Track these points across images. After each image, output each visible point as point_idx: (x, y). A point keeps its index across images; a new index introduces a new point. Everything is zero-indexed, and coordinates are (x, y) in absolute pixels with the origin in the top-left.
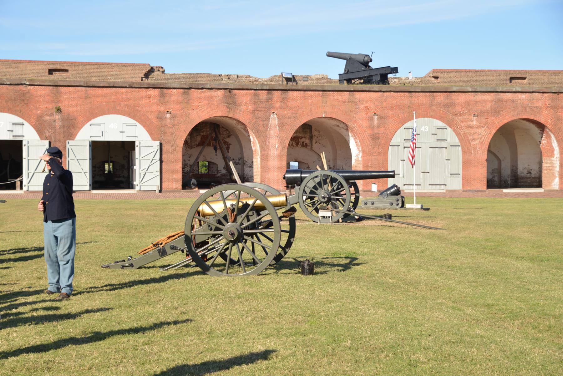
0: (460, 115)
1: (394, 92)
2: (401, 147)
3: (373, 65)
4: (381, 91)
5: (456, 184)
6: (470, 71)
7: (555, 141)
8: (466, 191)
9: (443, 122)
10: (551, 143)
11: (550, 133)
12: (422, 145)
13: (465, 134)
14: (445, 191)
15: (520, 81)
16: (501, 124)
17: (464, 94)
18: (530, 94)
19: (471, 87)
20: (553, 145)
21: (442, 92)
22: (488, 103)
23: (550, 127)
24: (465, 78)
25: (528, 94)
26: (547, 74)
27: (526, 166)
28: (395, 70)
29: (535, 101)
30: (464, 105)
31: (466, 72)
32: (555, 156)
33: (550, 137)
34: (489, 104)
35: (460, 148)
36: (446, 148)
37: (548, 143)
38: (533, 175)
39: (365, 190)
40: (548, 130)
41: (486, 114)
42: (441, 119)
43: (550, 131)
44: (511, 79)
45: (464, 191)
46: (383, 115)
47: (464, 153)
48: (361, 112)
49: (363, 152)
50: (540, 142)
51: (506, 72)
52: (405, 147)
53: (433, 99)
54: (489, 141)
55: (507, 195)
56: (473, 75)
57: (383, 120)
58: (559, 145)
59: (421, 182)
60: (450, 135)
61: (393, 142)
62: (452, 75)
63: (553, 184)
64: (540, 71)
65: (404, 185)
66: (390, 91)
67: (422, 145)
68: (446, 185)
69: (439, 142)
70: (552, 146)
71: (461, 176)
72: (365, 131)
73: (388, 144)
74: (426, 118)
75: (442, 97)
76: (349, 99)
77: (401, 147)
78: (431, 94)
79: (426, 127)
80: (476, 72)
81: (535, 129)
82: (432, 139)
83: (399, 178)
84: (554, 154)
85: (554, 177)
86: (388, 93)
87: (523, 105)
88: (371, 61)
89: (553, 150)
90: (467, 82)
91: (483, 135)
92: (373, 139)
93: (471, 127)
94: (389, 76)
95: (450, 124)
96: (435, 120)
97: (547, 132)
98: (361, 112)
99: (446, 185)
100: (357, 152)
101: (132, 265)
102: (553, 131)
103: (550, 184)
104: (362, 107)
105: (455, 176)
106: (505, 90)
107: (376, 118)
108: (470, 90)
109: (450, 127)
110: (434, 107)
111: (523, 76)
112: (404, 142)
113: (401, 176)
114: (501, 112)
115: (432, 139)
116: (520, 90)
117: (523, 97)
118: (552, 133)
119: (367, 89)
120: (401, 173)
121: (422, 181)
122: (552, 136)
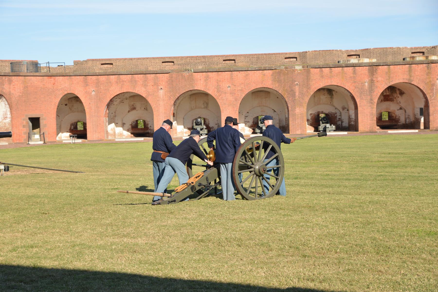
101: (175, 201)
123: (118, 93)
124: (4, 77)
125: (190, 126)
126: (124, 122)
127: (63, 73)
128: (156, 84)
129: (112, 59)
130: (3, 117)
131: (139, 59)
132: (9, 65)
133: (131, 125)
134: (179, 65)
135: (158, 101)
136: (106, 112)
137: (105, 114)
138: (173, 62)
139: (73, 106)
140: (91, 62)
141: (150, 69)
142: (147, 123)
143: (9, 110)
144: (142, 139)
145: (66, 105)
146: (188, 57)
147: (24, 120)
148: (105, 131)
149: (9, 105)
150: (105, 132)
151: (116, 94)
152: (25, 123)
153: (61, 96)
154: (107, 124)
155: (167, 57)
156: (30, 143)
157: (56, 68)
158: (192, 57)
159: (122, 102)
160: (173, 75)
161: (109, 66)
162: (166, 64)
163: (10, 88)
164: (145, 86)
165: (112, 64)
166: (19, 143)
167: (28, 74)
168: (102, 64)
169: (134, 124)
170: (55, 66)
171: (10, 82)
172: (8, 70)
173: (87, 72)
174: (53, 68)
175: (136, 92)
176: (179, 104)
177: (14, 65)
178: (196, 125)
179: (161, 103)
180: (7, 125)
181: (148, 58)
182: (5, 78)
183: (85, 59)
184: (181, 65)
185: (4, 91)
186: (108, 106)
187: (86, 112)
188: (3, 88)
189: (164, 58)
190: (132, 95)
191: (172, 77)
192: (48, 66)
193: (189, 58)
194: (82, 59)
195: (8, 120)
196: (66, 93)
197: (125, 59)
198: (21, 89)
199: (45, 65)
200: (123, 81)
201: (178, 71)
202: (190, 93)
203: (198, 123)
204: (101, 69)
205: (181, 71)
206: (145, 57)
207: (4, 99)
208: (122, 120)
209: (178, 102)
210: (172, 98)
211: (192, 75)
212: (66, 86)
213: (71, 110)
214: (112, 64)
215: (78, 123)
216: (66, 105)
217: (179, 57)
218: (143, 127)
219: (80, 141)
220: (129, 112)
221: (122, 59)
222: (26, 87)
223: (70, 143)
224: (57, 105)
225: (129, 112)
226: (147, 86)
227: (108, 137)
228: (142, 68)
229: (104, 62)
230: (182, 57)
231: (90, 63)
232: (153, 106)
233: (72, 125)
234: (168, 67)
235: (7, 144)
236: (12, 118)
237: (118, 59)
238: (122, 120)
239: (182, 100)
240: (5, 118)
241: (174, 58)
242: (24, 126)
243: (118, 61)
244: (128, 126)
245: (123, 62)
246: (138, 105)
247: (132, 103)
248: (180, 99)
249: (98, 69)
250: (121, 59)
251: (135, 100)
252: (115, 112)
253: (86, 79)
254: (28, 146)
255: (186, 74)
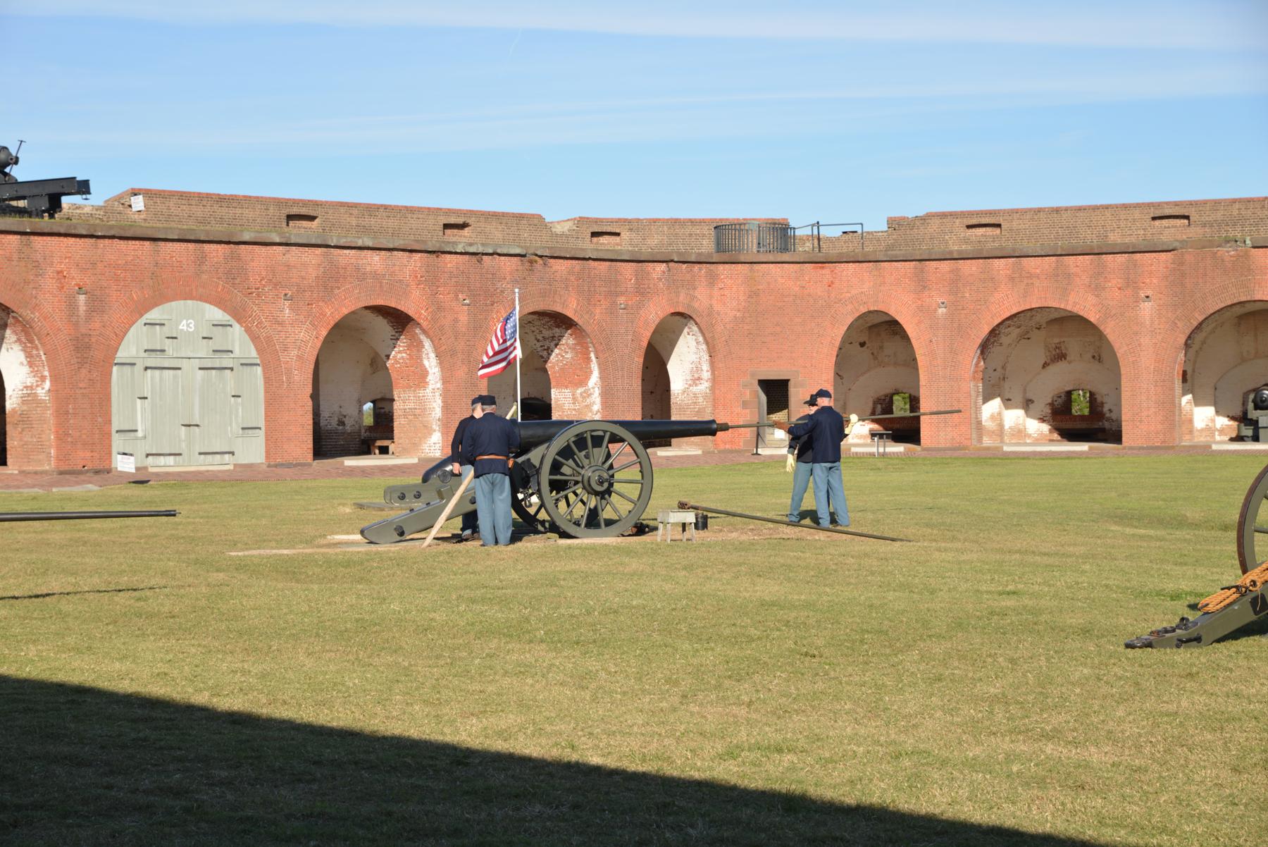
0: (258, 295)
1: (121, 238)
2: (139, 368)
3: (19, 173)
4: (92, 236)
5: (253, 452)
6: (208, 196)
7: (432, 355)
8: (276, 466)
9: (225, 310)
10: (420, 358)
11: (422, 337)
12: (184, 364)
13: (269, 338)
14: (231, 467)
15: (305, 223)
16: (337, 318)
17: (263, 249)
18: (388, 254)
19: (280, 234)
20: (426, 363)
21: (205, 240)
22: (310, 270)
23: (424, 324)
24: (199, 211)
25: (383, 253)
26: (355, 212)
27: (336, 408)
28: (83, 187)
29: (397, 268)
30: (264, 273)
31: (202, 198)
32: (431, 387)
33: (420, 345)
34: (313, 273)
35: (259, 370)
36: (232, 369)
37: (411, 357)
38: (348, 428)
39: (64, 468)
40: (418, 331)
41: (308, 294)
42: (219, 303)
43: (424, 332)
44: (290, 218)
45: (269, 466)
46: (98, 293)
47: (267, 381)
48: (49, 283)
49: (54, 379)
50: (388, 357)
51: (279, 202)
52: (146, 368)
53: (201, 260)
54: (315, 353)
55: (352, 471)
56: (216, 207)
57: (97, 304)
58: (441, 363)
59: (183, 448)
60: (238, 340)
61: (123, 354)
62: (171, 204)
63: (425, 447)
64: (342, 204)
65: (148, 455)
66: (113, 237)
67: (184, 364)
68: (233, 453)
69: (218, 355)
70: (423, 366)
71: (262, 433)
72: (59, 329)
73: (108, 361)
74: (189, 302)
75: (220, 253)
76: (20, 252)
77: (139, 368)
78: (198, 246)
79: (190, 319)
80: (221, 199)
81: (383, 327)
82: (204, 350)
83: (137, 438)
84: (427, 383)
85: (430, 432)
86: (107, 241)
87: (375, 275)
88: (16, 161)
89: (424, 373)
90: (203, 221)
91: (304, 340)
92: (77, 349)
93: (281, 324)
94: (66, 201)
95: (239, 315)
96: (207, 306)
97: (414, 338)
98: (49, 283)
99: (233, 453)
100: (30, 381)
101: (1198, 639)
102: (431, 333)
103: (415, 446)
104: (50, 272)
105: (250, 431)
106: (342, 242)
107: (82, 298)
108: (277, 240)
109: (238, 321)
110: (204, 277)
111: (312, 213)
112: (146, 355)
113: (140, 434)
114: (336, 291)
115: (204, 350)
116: (370, 244)
117: (376, 259)
118: (428, 336)
119: (62, 231)
120: (139, 429)
121: (184, 445)
122: (427, 344)
123: (1014, 312)
124: (697, 267)
125: (1238, 412)
126: (1030, 395)
127: (859, 252)
128: (1131, 283)
129: (999, 211)
130: (689, 377)
131: (1080, 209)
132: (709, 232)
133: (1051, 404)
134: (1204, 225)
135: (1136, 333)
136: (977, 365)
137: (975, 372)
138: (1187, 217)
139: (881, 348)
140: (937, 221)
141: (1115, 238)
142: (1099, 399)
143: (706, 357)
144: (1083, 447)
145: (862, 345)
146: (1234, 201)
147: (745, 386)
148: (973, 421)
149: (707, 343)
150: (974, 426)
151: (1008, 315)
152: (748, 395)
153: (850, 320)
154: (980, 400)
155: (1167, 203)
156: (760, 451)
157: (838, 239)
158: (1249, 200)
159: (1025, 336)
160: (1187, 257)
161: (989, 231)
162: (1165, 222)
163: (711, 297)
164: (1096, 288)
165: (999, 226)
166: (731, 451)
167: (762, 258)
168: (969, 227)
169: (1060, 401)
170: (836, 232)
171: (712, 280)
172: (707, 246)
173: (923, 249)
174: (829, 239)
175: (1069, 308)
176: (1203, 343)
177: (722, 229)
178: (1257, 407)
179: (1146, 340)
180: (701, 400)
181: (1107, 207)
182: (700, 269)
183: (921, 213)
184: (1212, 226)
185: (696, 305)
186: (984, 347)
187: (920, 364)
188: (693, 298)
189: (1159, 205)
190: (1056, 315)
191: (1182, 264)
192: (815, 232)
193: (1237, 206)
194: (911, 215)
195: (704, 386)
196: (863, 310)
197: (1039, 210)
198: (742, 298)
199: (808, 231)
200: (1031, 276)
201: (1204, 245)
202: (1239, 311)
203: (1263, 401)
204: (966, 241)
205: (1211, 244)
206: (1099, 203)
207: (695, 328)
208: (1025, 390)
209: (1199, 338)
210: (1179, 324)
211: (1246, 255)
212: (863, 291)
213: (876, 358)
214: (999, 226)
215: (895, 398)
216: (862, 345)
217: (1205, 202)
218: (1086, 412)
219: (899, 448)
220: (1045, 365)
221: (1030, 210)
222: (753, 294)
223: (872, 455)
224: (837, 344)
225: (1045, 365)
226: (1104, 289)
227: (980, 440)
228: (1090, 238)
229: (974, 221)
230: (1216, 203)
231: (935, 225)
232: (1120, 347)
233: (877, 401)
234: (1170, 232)
235: (700, 452)
236: (714, 380)
237: (1017, 211)
238: (1025, 390)
239: (1213, 331)
240: (697, 380)
241: (1191, 203)
242: (745, 405)
243: (1016, 216)
244: (1042, 406)
245: (1032, 219)
246: (1073, 346)
247: (1056, 340)
248: (1207, 329)
249: (958, 240)
250: (1024, 212)
251: (1065, 332)
252: (1004, 368)
253: (922, 271)
254: (755, 459)
255: (1228, 252)
